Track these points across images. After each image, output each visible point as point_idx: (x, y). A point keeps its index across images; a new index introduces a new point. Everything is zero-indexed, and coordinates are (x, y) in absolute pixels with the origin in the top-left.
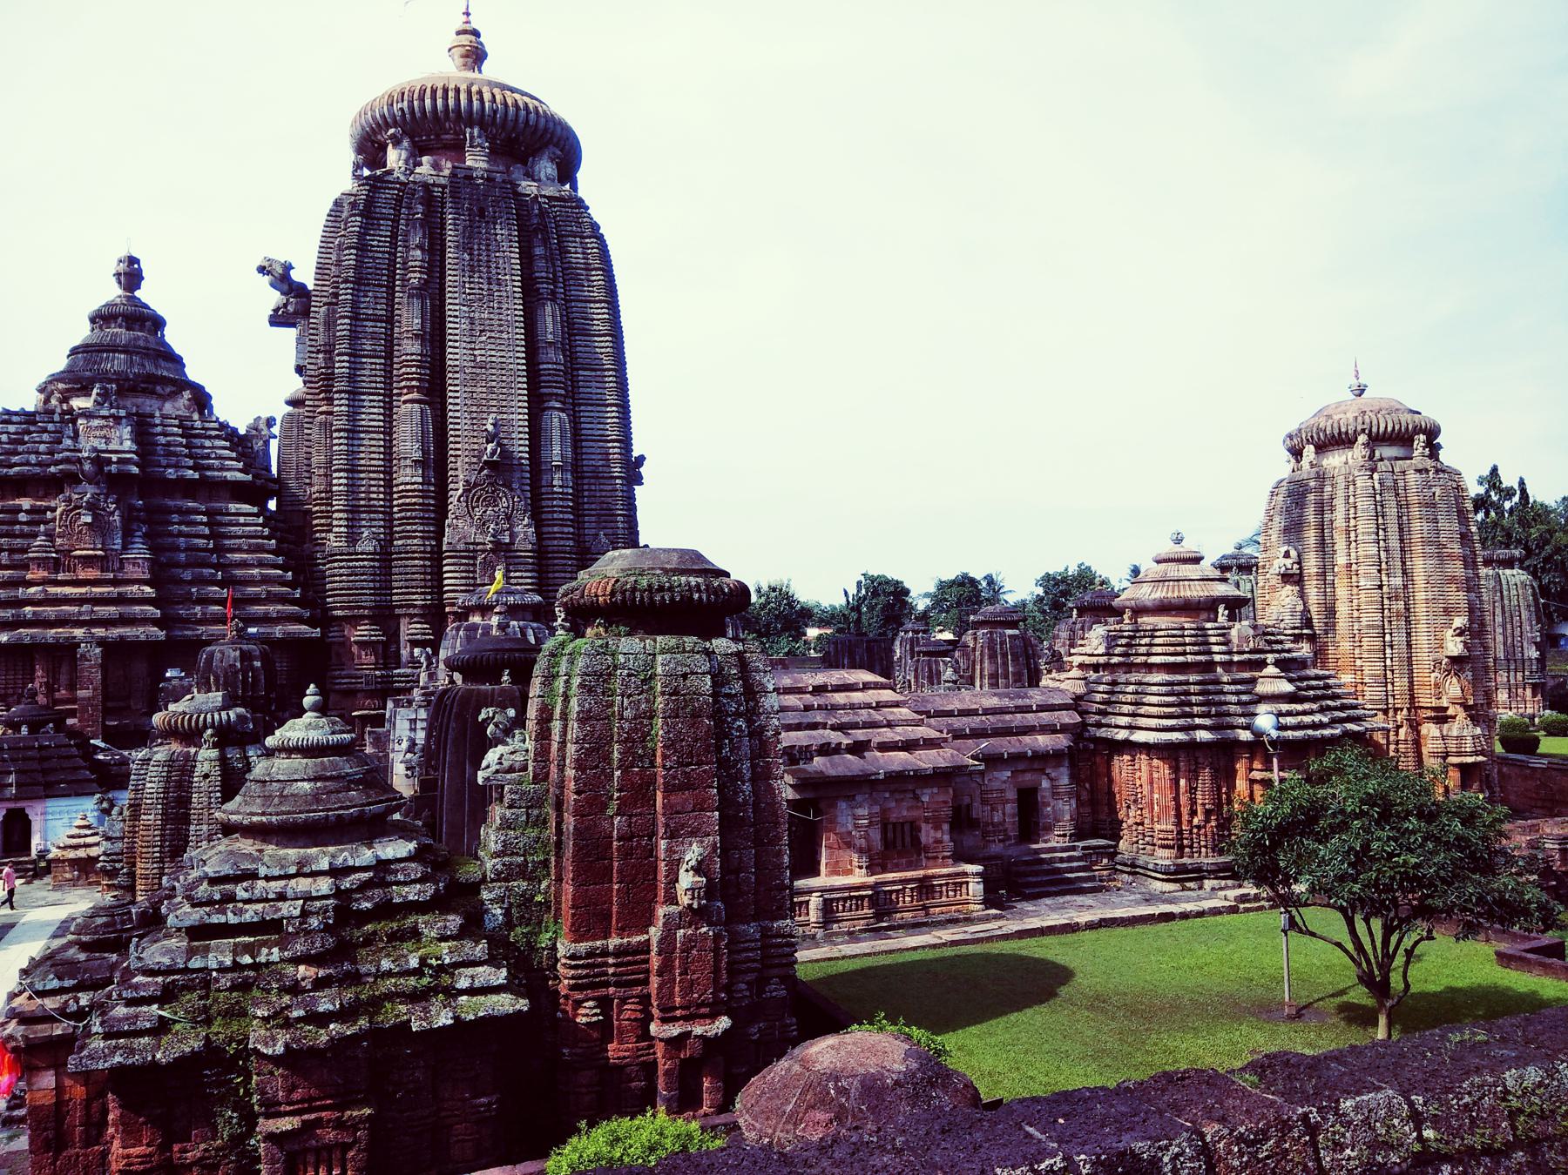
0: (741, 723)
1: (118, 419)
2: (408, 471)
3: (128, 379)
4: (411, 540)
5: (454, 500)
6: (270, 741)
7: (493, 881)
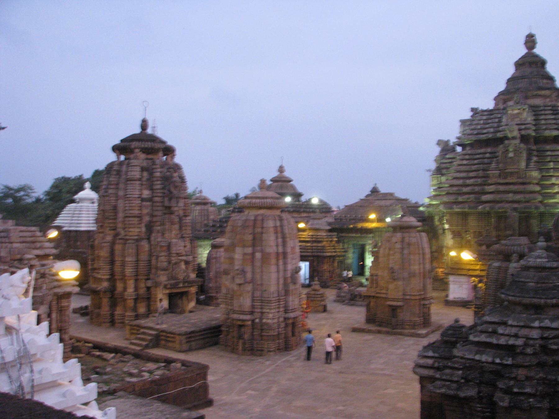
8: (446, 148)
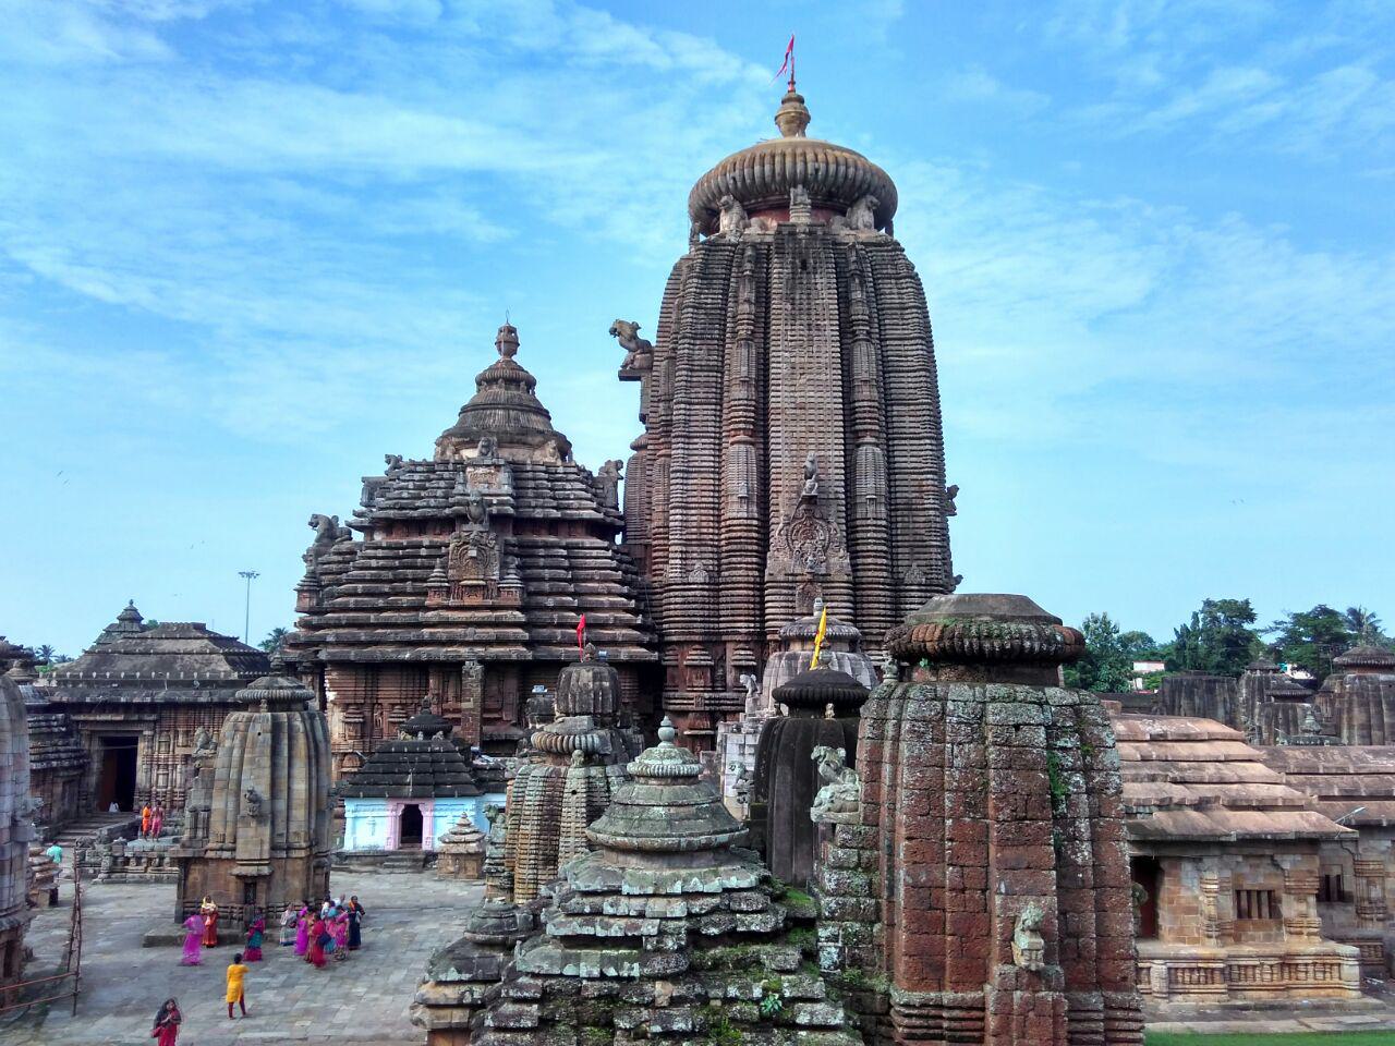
0: (1078, 778)
1: (497, 467)
2: (736, 507)
3: (506, 432)
4: (741, 573)
5: (775, 533)
6: (632, 768)
7: (827, 919)
8: (329, 531)
